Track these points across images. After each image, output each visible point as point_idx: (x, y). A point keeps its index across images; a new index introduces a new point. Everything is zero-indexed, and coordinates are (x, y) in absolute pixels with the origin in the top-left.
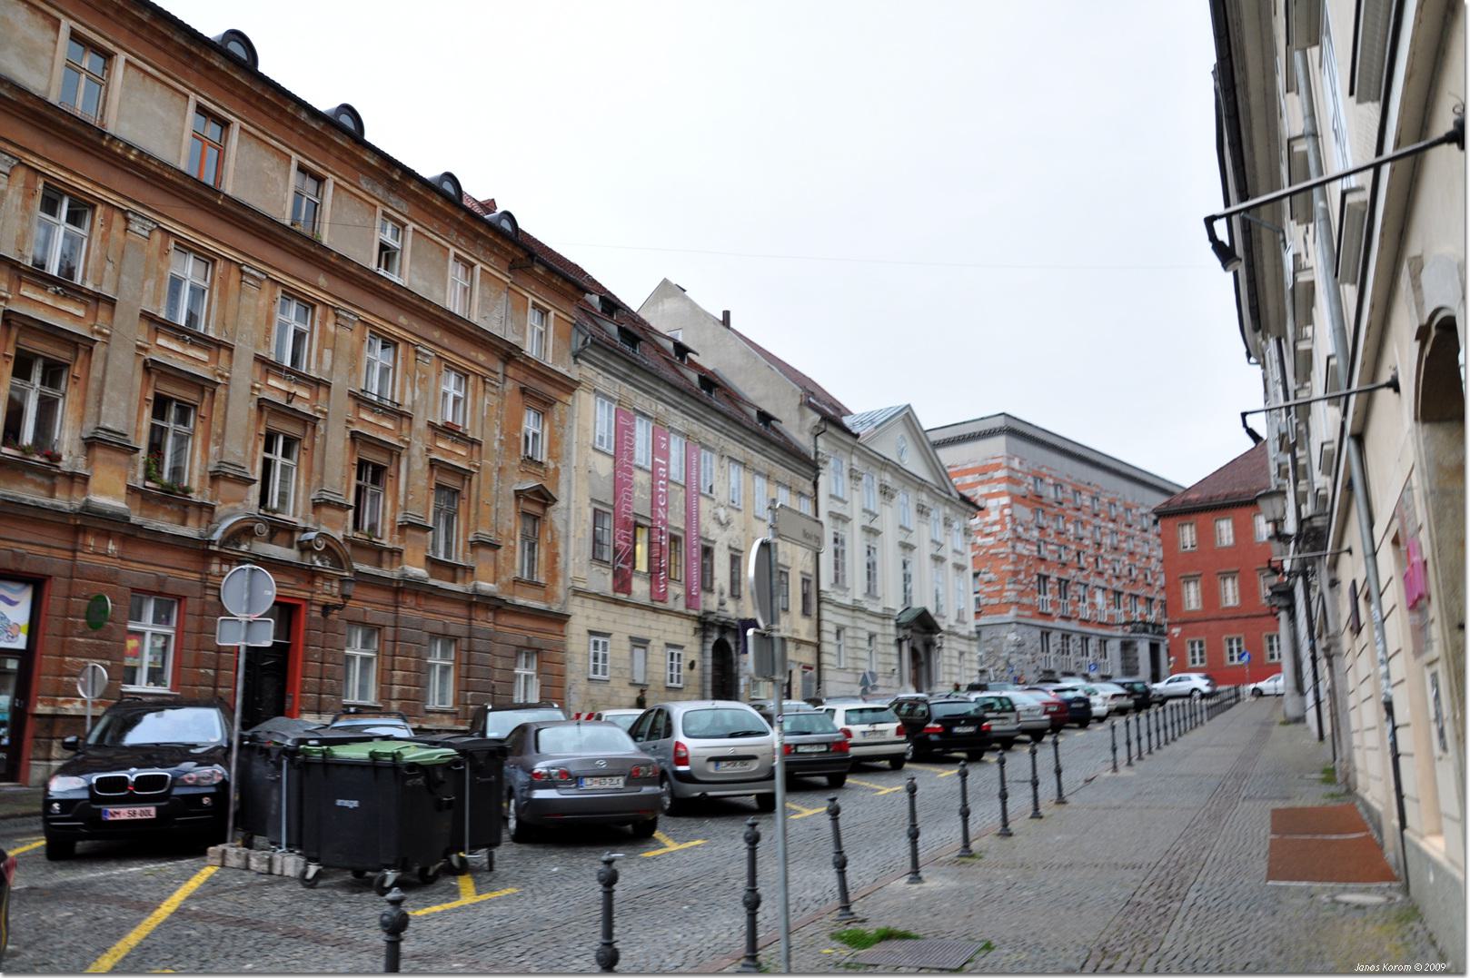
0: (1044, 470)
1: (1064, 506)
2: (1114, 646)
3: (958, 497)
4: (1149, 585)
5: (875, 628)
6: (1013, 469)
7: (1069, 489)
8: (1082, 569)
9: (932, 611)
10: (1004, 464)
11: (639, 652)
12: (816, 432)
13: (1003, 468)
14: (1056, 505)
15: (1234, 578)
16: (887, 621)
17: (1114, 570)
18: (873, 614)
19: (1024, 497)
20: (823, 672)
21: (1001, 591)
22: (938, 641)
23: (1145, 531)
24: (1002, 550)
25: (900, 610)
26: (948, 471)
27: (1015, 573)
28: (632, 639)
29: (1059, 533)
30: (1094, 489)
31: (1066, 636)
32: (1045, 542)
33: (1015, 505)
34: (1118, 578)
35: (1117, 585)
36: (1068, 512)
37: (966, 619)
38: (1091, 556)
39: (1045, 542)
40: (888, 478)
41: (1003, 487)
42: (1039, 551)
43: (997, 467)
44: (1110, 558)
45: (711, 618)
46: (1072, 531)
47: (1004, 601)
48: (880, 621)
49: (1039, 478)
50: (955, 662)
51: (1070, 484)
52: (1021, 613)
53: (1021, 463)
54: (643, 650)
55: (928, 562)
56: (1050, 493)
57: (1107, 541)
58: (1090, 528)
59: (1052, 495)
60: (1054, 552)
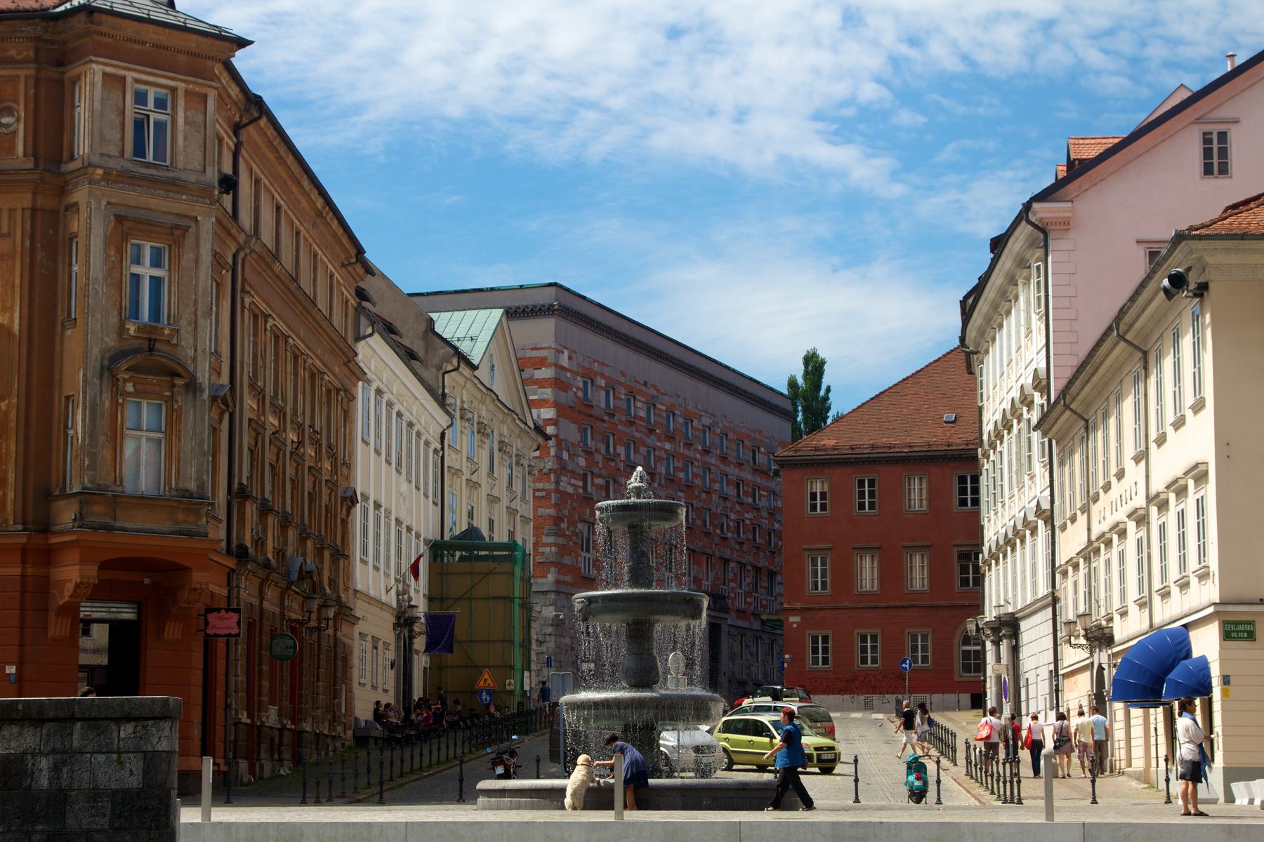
3: (532, 426)
4: (707, 534)
6: (562, 367)
10: (551, 360)
13: (545, 366)
14: (606, 418)
19: (573, 408)
27: (557, 520)
32: (592, 473)
33: (563, 422)
36: (620, 427)
39: (592, 473)
41: (548, 393)
42: (585, 487)
43: (540, 363)
51: (624, 385)
52: (562, 578)
53: (570, 358)
56: (599, 399)
57: (662, 469)
58: (643, 450)
59: (603, 405)
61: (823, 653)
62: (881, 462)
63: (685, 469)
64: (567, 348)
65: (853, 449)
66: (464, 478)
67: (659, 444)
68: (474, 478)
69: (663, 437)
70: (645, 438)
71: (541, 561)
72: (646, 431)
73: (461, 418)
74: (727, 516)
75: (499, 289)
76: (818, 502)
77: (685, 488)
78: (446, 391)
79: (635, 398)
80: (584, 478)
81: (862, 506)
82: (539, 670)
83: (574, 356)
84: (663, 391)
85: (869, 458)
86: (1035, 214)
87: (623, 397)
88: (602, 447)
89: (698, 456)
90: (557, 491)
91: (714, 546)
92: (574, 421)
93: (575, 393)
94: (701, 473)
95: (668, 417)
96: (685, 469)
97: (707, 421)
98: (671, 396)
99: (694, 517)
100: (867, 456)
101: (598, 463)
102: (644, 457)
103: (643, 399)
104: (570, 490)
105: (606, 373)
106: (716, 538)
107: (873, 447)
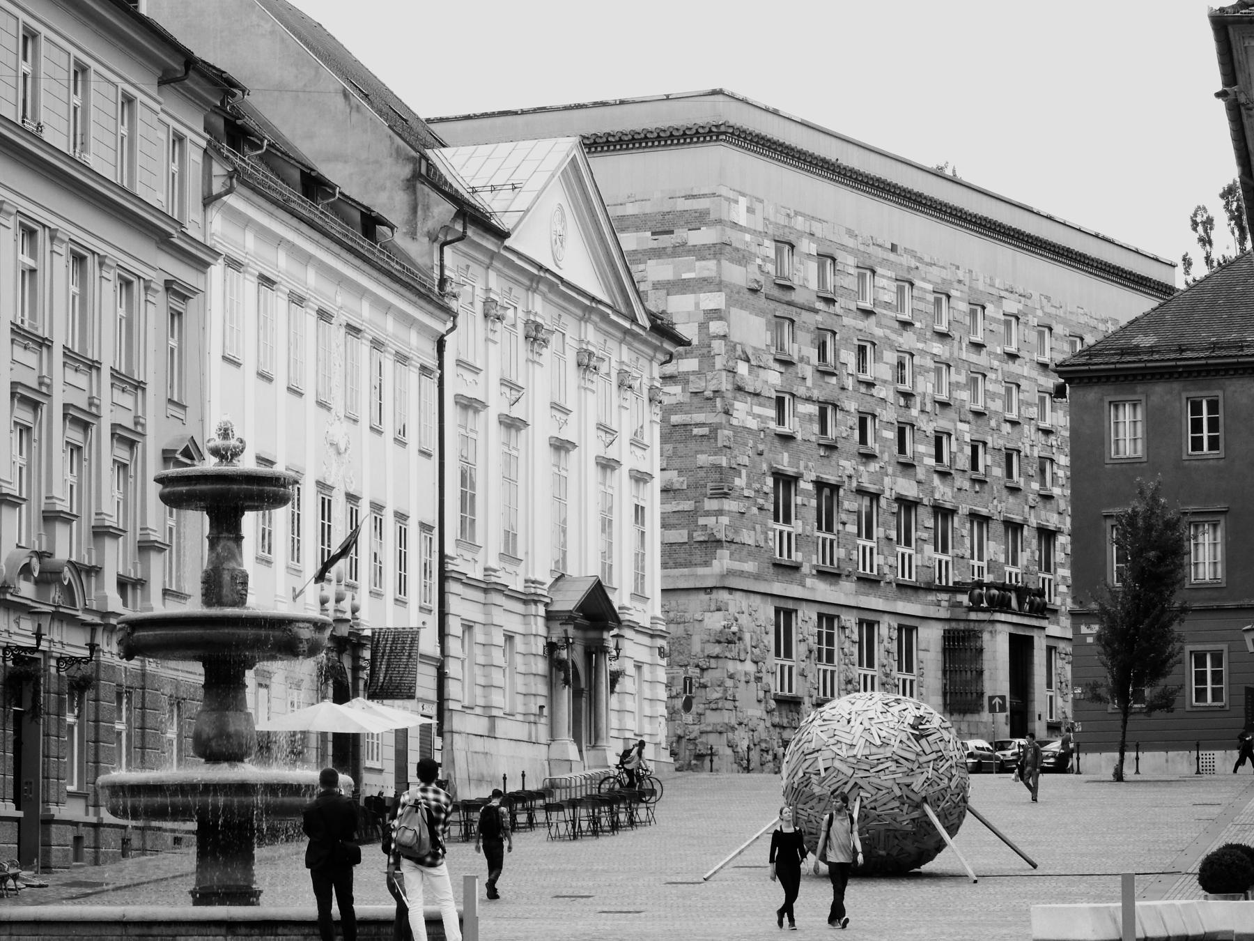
0: (800, 223)
1: (837, 308)
2: (930, 638)
3: (648, 325)
4: (1014, 490)
5: (514, 624)
8: (869, 457)
11: (263, 691)
12: (441, 238)
13: (706, 224)
14: (820, 305)
15: (1215, 526)
17: (939, 457)
18: (512, 595)
20: (447, 714)
21: (693, 515)
22: (611, 644)
23: (1013, 357)
24: (699, 417)
25: (549, 581)
31: (828, 619)
33: (736, 314)
34: (944, 475)
35: (943, 492)
36: (846, 321)
37: (647, 594)
39: (793, 395)
40: (540, 308)
42: (781, 420)
47: (699, 536)
48: (479, 596)
50: (498, 657)
52: (737, 566)
53: (750, 210)
56: (806, 275)
57: (925, 386)
58: (891, 357)
59: (813, 284)
61: (1213, 682)
62: (1227, 371)
64: (743, 195)
65: (1181, 351)
66: (492, 414)
67: (920, 346)
68: (517, 412)
69: (929, 334)
70: (893, 336)
71: (702, 539)
72: (897, 325)
73: (486, 316)
74: (1052, 461)
75: (634, 102)
76: (1205, 434)
77: (970, 417)
78: (447, 273)
79: (874, 272)
80: (780, 402)
81: (1197, 444)
82: (701, 715)
83: (758, 206)
84: (927, 259)
85: (1207, 365)
87: (852, 271)
88: (813, 354)
89: (996, 364)
91: (1027, 508)
92: (761, 313)
93: (760, 266)
94: (1003, 391)
95: (938, 302)
97: (1012, 306)
98: (944, 267)
99: (989, 463)
100: (1203, 362)
101: (804, 379)
102: (891, 365)
103: (889, 274)
104: (753, 424)
105: (819, 234)
106: (1031, 497)
107: (1215, 346)
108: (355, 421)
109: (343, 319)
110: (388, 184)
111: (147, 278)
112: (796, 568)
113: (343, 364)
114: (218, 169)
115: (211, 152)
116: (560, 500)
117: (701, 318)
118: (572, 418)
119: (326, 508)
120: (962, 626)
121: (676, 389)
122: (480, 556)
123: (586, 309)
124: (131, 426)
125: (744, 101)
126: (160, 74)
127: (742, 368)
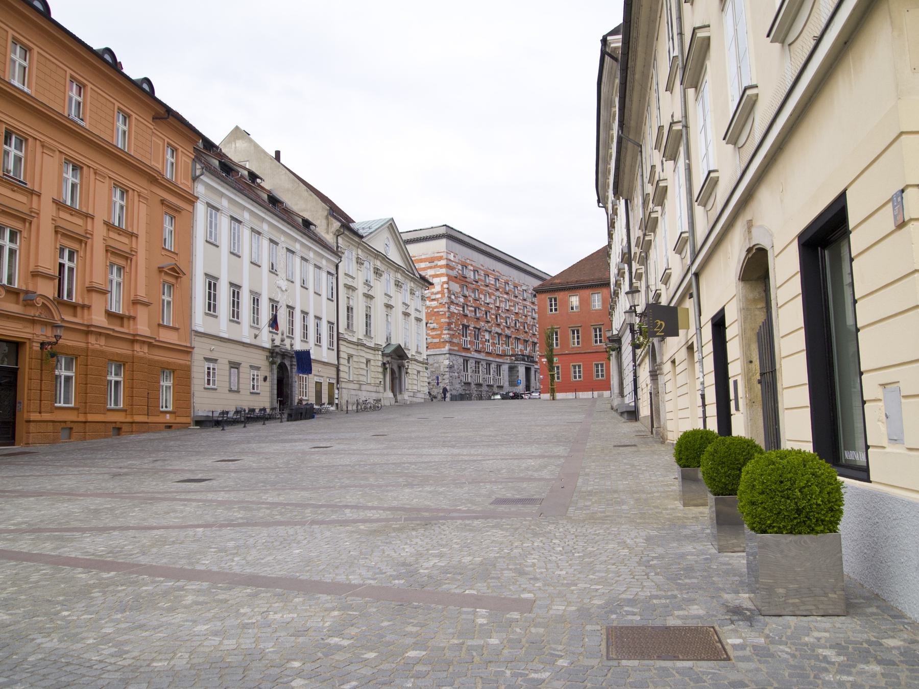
0: (468, 261)
1: (479, 284)
2: (505, 368)
5: (370, 357)
6: (450, 260)
7: (482, 273)
8: (488, 322)
9: (403, 346)
10: (445, 257)
11: (234, 371)
12: (337, 234)
13: (443, 259)
14: (474, 283)
16: (377, 352)
17: (506, 323)
19: (456, 277)
22: (406, 364)
23: (525, 300)
24: (441, 309)
25: (384, 345)
26: (413, 259)
27: (449, 324)
28: (230, 362)
29: (476, 300)
30: (497, 274)
31: (478, 362)
33: (451, 283)
34: (508, 328)
35: (508, 332)
36: (481, 287)
38: (493, 314)
39: (467, 305)
40: (378, 264)
41: (444, 271)
42: (464, 311)
43: (441, 258)
44: (504, 316)
45: (277, 350)
46: (483, 299)
47: (442, 340)
48: (372, 352)
49: (465, 266)
52: (452, 348)
53: (454, 257)
54: (236, 370)
55: (401, 316)
56: (470, 275)
57: (503, 305)
59: (472, 277)
60: (471, 311)
63: (514, 306)
83: (457, 256)
86: (610, 43)
90: (449, 311)
96: (514, 306)
97: (524, 288)
106: (530, 335)
108: (292, 282)
109: (284, 246)
110: (320, 217)
111: (95, 168)
112: (469, 349)
113: (285, 261)
114: (198, 166)
115: (196, 160)
116: (332, 293)
117: (441, 284)
118: (392, 299)
119: (256, 301)
120: (513, 365)
121: (436, 302)
122: (356, 335)
123: (397, 268)
124: (129, 252)
125: (452, 228)
126: (154, 114)
127: (453, 297)
